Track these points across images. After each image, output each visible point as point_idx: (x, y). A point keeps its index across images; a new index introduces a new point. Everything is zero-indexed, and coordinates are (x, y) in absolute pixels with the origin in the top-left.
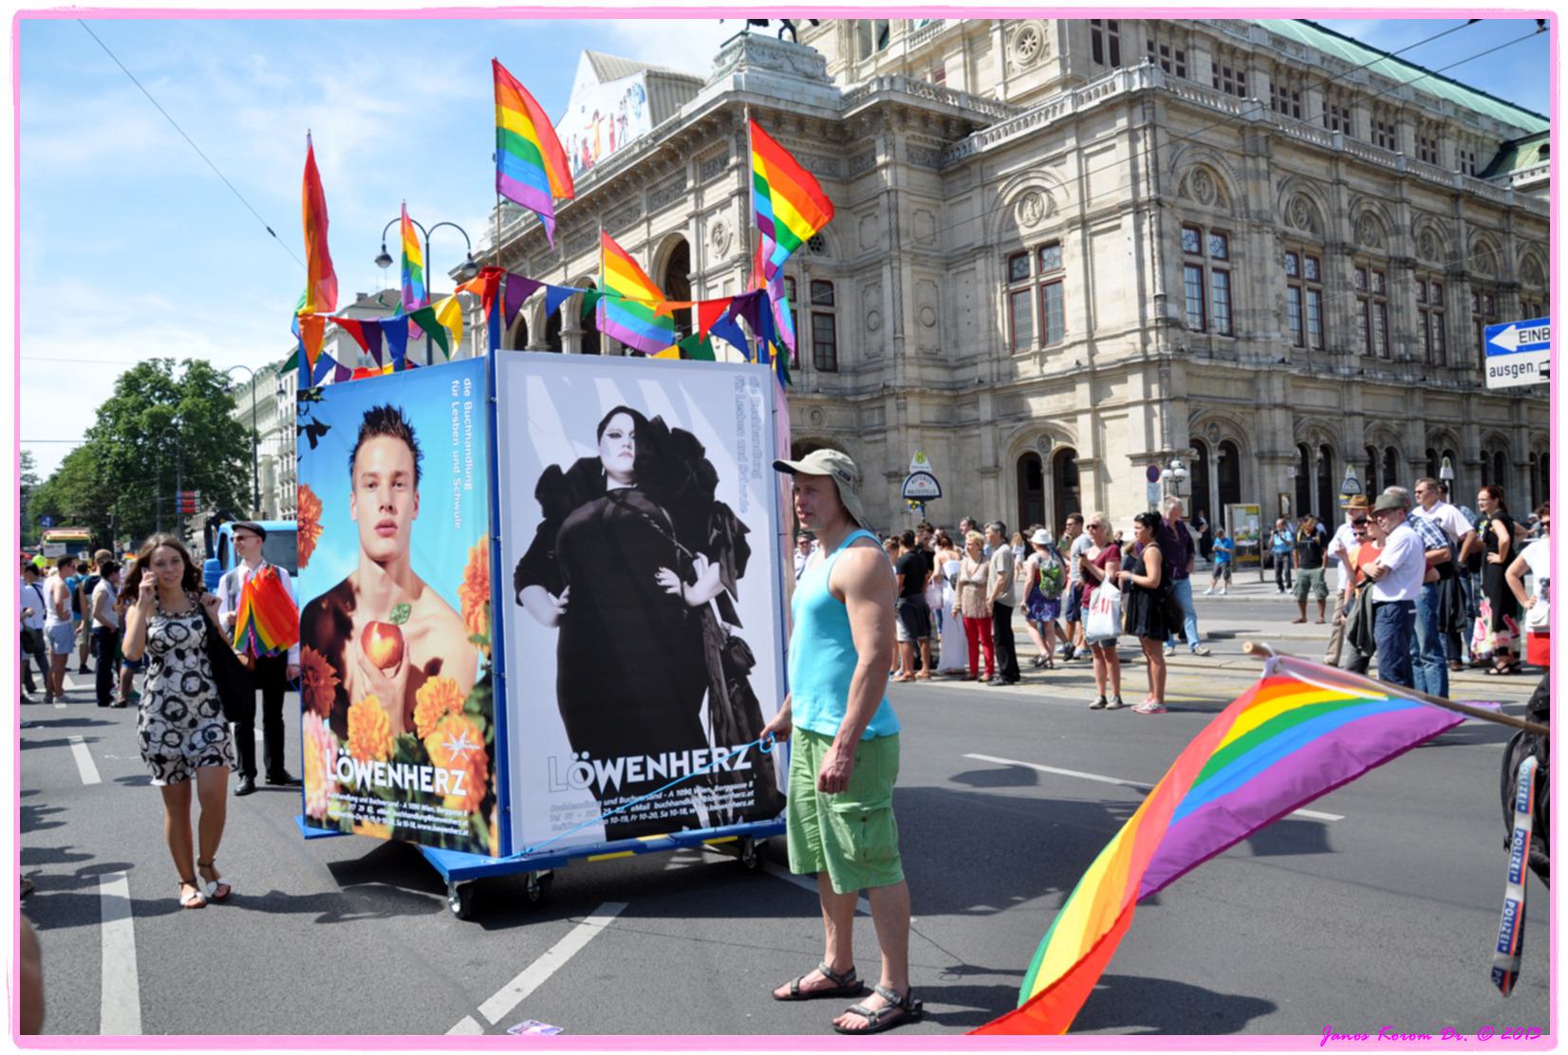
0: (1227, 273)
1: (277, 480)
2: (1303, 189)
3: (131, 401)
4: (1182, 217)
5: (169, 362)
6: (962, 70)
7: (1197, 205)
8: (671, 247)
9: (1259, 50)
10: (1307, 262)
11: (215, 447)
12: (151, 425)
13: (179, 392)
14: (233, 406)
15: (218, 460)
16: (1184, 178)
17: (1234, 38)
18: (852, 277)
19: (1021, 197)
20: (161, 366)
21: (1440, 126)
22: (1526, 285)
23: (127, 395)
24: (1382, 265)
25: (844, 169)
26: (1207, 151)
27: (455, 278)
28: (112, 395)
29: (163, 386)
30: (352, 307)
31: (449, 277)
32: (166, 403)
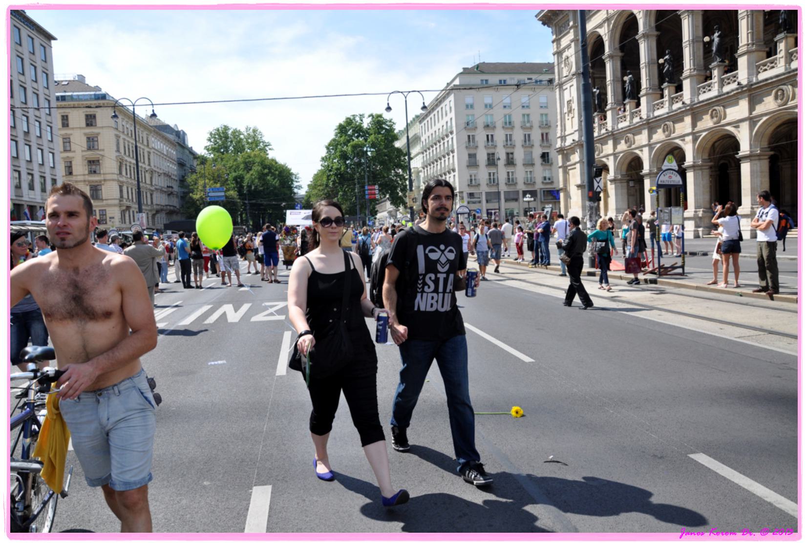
1: (422, 181)
3: (342, 139)
5: (362, 116)
11: (387, 162)
12: (353, 151)
13: (367, 132)
14: (396, 138)
15: (389, 170)
20: (358, 119)
23: (341, 137)
27: (540, 20)
28: (332, 136)
29: (359, 130)
30: (461, 73)
31: (536, 19)
32: (361, 139)
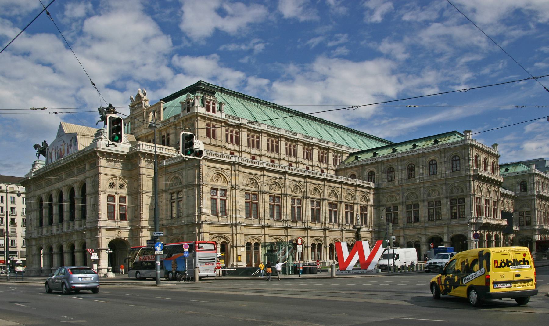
0: (225, 200)
2: (252, 177)
4: (211, 187)
6: (173, 135)
7: (216, 183)
8: (83, 184)
9: (262, 131)
10: (253, 196)
16: (213, 177)
17: (255, 128)
18: (131, 196)
19: (174, 178)
21: (328, 149)
22: (331, 199)
24: (280, 196)
25: (130, 167)
26: (220, 170)
